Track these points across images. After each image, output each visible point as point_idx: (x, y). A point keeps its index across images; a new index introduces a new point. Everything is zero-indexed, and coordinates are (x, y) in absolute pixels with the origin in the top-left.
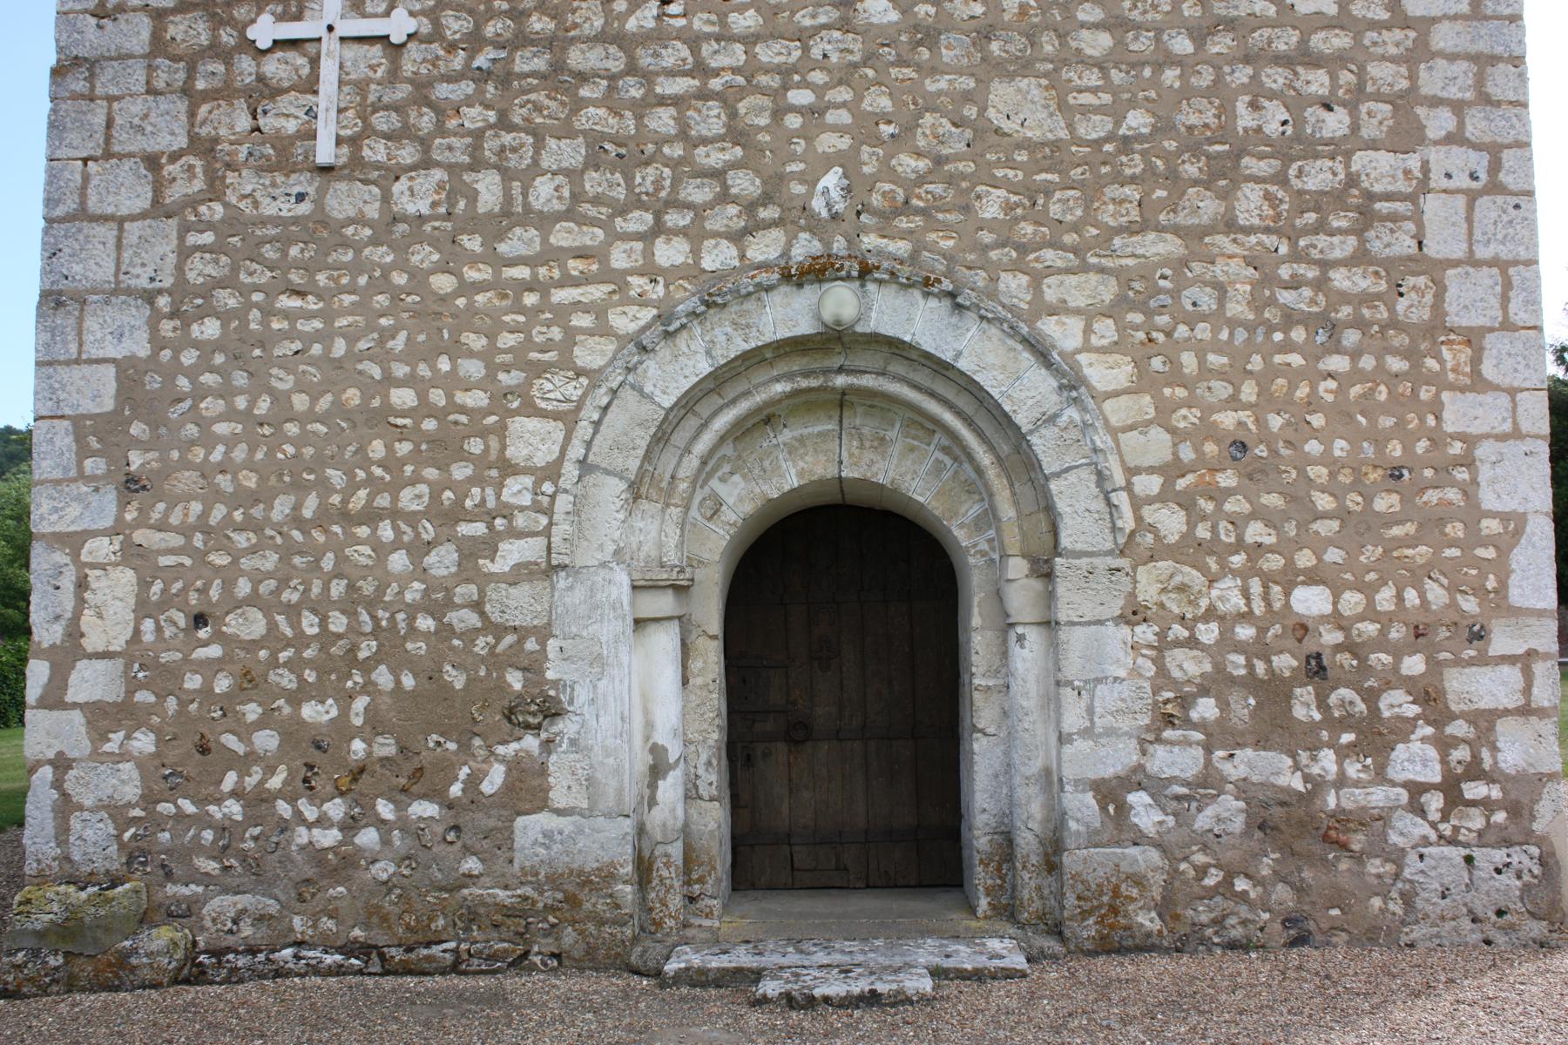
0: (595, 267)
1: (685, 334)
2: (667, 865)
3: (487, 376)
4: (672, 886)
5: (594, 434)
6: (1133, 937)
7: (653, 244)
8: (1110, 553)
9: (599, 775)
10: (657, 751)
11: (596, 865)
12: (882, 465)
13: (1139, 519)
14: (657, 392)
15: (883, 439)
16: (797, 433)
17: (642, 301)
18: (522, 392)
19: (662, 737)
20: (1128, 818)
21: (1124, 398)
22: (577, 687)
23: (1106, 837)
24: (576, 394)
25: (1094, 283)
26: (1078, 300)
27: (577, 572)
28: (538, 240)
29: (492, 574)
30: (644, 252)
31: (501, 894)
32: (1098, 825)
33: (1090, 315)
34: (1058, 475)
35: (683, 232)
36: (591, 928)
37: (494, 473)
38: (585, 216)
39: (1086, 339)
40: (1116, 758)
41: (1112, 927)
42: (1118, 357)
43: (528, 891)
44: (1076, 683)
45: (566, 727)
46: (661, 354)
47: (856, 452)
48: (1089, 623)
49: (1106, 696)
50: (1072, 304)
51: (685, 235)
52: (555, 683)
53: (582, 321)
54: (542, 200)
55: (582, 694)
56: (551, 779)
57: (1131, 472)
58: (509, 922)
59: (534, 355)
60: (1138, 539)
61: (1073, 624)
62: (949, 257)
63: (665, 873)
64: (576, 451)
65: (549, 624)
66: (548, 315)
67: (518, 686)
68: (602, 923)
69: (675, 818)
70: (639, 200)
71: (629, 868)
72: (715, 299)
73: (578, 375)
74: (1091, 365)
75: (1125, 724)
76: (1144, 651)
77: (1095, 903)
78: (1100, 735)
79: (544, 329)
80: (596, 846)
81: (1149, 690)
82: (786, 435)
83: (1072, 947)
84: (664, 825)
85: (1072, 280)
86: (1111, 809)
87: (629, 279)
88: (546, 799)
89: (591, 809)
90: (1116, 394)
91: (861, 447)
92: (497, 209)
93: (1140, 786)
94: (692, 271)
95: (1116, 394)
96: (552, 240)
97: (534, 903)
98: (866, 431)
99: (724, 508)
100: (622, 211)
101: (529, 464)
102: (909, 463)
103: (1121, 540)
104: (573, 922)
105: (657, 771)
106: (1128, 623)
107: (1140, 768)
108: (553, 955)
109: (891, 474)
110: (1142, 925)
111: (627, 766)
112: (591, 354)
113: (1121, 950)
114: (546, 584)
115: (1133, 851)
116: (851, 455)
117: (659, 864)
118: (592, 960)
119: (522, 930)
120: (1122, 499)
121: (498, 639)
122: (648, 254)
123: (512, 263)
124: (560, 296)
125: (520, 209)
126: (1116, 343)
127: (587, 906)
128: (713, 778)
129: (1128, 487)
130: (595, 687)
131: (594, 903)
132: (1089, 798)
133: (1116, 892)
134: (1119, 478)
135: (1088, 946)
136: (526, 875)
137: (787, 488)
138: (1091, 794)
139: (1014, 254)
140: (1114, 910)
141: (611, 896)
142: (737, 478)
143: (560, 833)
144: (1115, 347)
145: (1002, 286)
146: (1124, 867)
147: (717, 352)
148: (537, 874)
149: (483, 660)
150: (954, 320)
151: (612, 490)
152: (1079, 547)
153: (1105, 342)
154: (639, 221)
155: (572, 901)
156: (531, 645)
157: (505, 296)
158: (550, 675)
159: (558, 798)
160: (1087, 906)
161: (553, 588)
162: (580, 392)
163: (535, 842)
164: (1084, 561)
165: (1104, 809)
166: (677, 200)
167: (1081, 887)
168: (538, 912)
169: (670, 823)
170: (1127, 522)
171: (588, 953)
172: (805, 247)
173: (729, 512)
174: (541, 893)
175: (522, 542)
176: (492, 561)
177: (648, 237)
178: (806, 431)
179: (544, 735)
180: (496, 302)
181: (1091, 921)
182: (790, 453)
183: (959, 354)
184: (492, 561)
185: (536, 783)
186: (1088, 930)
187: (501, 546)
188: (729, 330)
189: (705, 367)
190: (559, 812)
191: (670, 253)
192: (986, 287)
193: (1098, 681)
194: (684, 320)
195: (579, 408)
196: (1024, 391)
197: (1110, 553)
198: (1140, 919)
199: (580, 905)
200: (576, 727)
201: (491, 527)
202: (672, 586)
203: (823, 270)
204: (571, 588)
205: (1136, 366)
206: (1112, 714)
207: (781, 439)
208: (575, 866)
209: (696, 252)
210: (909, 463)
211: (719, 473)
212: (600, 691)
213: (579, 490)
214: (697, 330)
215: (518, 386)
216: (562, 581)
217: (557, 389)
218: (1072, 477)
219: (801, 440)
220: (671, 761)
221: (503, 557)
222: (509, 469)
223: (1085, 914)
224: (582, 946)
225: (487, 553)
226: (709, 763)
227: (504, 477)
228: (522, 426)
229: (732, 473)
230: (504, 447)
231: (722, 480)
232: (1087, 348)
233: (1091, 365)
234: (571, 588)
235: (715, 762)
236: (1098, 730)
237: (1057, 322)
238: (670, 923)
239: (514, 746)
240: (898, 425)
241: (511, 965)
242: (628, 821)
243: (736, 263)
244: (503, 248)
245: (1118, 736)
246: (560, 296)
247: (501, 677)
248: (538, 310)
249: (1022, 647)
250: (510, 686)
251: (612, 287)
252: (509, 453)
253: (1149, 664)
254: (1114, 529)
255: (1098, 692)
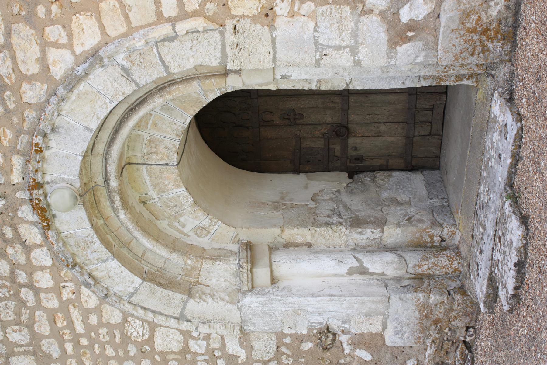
0: (60, 315)
1: (95, 274)
2: (420, 266)
3: (132, 360)
4: (434, 263)
5: (161, 314)
6: (507, 18)
7: (40, 288)
8: (222, 34)
9: (364, 311)
10: (351, 272)
11: (417, 313)
12: (167, 142)
13: (195, 14)
14: (133, 285)
15: (150, 141)
16: (151, 188)
17: (77, 293)
18: (140, 345)
19: (344, 270)
20: (418, 22)
21: (104, 21)
22: (312, 321)
23: (431, 38)
24: (138, 323)
25: (19, 40)
26: (35, 51)
27: (245, 321)
28: (48, 340)
29: (247, 357)
30: (46, 293)
31: (429, 352)
32: (421, 44)
33: (45, 46)
34: (166, 68)
35: (30, 275)
36: (453, 314)
37: (188, 356)
38: (29, 320)
39: (63, 46)
40: (374, 30)
41: (496, 33)
42: (73, 26)
43: (428, 342)
44: (317, 57)
45: (335, 325)
46: (109, 285)
47: (159, 156)
48: (274, 48)
49: (328, 36)
50: (39, 55)
51: (31, 274)
52: (309, 330)
53: (94, 320)
54: (23, 338)
55: (317, 318)
56: (365, 332)
57: (160, 18)
58: (445, 347)
59: (118, 340)
60: (211, 13)
61: (274, 58)
62: (18, 133)
63: (425, 267)
64: (173, 323)
65: (276, 333)
66: (93, 334)
67: (311, 345)
68: (452, 309)
69: (392, 262)
70: (14, 295)
71: (420, 295)
72: (67, 262)
73: (127, 321)
74: (82, 44)
75: (349, 24)
76: (296, 9)
77: (478, 44)
78: (356, 42)
79: (101, 336)
80: (406, 312)
81: (324, 8)
82: (153, 193)
83: (507, 58)
84: (396, 269)
85: (20, 55)
86: (410, 34)
87: (64, 299)
88: (377, 334)
89: (384, 315)
90: (102, 27)
91: (156, 153)
92: (33, 358)
93: (396, 14)
94: (54, 270)
95: (102, 27)
96: (47, 334)
97: (436, 339)
98: (145, 150)
99: (201, 225)
100: (23, 303)
101: (182, 341)
102: (164, 126)
103: (212, 26)
104: (449, 321)
105: (363, 271)
106: (273, 20)
107: (382, 14)
108: (467, 330)
109: (173, 137)
110: (499, 12)
111: (360, 298)
112: (113, 315)
113: (515, 27)
114: (251, 334)
115: (444, 19)
116: (162, 159)
117: (420, 271)
118: (472, 313)
119: (451, 343)
120: (182, 27)
121: (284, 354)
122: (47, 290)
123: (64, 350)
124: (80, 328)
125: (31, 348)
126: (64, 26)
127: (440, 316)
128: (369, 231)
129: (173, 21)
130: (312, 313)
131: (439, 313)
132: (402, 49)
133: (472, 31)
134: (165, 30)
135: (508, 47)
136: (419, 342)
137: (186, 194)
138: (398, 48)
139: (8, 93)
140: (486, 31)
141: (436, 305)
142: (182, 219)
143: (397, 327)
144: (67, 27)
145: (33, 101)
146: (454, 26)
147: (104, 257)
148: (420, 337)
149: (295, 360)
150: (63, 131)
151: (194, 307)
152: (218, 54)
153: (64, 34)
154: (27, 295)
155: (436, 322)
156: (287, 340)
157: (85, 353)
158: (305, 332)
159: (376, 328)
160: (479, 49)
161: (253, 332)
162: (137, 321)
163: (401, 338)
164: (228, 50)
165: (410, 39)
166: (10, 277)
167: (464, 54)
168: (441, 336)
169: (395, 265)
170: (199, 23)
171: (468, 315)
172: (26, 212)
173: (204, 223)
174: (430, 335)
175: (228, 345)
176: (239, 357)
177: (37, 292)
178: (149, 183)
179: (339, 333)
180: (88, 356)
181: (490, 45)
182: (164, 192)
183: (87, 129)
184: (239, 357)
185: (367, 338)
186: (496, 47)
187: (230, 352)
188: (89, 251)
189: (114, 263)
190: (385, 327)
191: (44, 280)
192: (36, 111)
193: (316, 42)
194: (86, 277)
195: (147, 321)
196: (105, 90)
197: (222, 34)
198: (494, 13)
199: (440, 319)
200: (335, 321)
201: (220, 357)
202: (251, 271)
203: (43, 210)
204: (254, 324)
205: (79, 13)
206: (341, 34)
207: (155, 196)
208: (416, 321)
209: (42, 268)
210: (164, 126)
211: (180, 228)
212: (315, 310)
213: (195, 322)
214: (92, 267)
215: (136, 347)
216: (249, 328)
217: (136, 330)
218: (168, 59)
219: (155, 186)
220: (358, 265)
221: (236, 353)
222: (185, 350)
223: (485, 50)
224: (464, 318)
225: (235, 359)
226: (360, 233)
227: (190, 352)
228: (159, 344)
229: (179, 221)
230: (173, 352)
231: (184, 226)
232: (70, 46)
233: (82, 44)
234: (254, 324)
235: (360, 230)
236: (352, 42)
237: (54, 66)
238: (455, 264)
239: (345, 345)
240: (139, 132)
241: (470, 352)
242: (392, 297)
243: (45, 249)
244: (56, 355)
245: (358, 29)
246: (80, 328)
247: (305, 352)
248: (90, 339)
249: (291, 76)
250: (310, 349)
251: (71, 306)
252: (176, 350)
253: (305, 6)
254: (205, 31)
255: (325, 43)
